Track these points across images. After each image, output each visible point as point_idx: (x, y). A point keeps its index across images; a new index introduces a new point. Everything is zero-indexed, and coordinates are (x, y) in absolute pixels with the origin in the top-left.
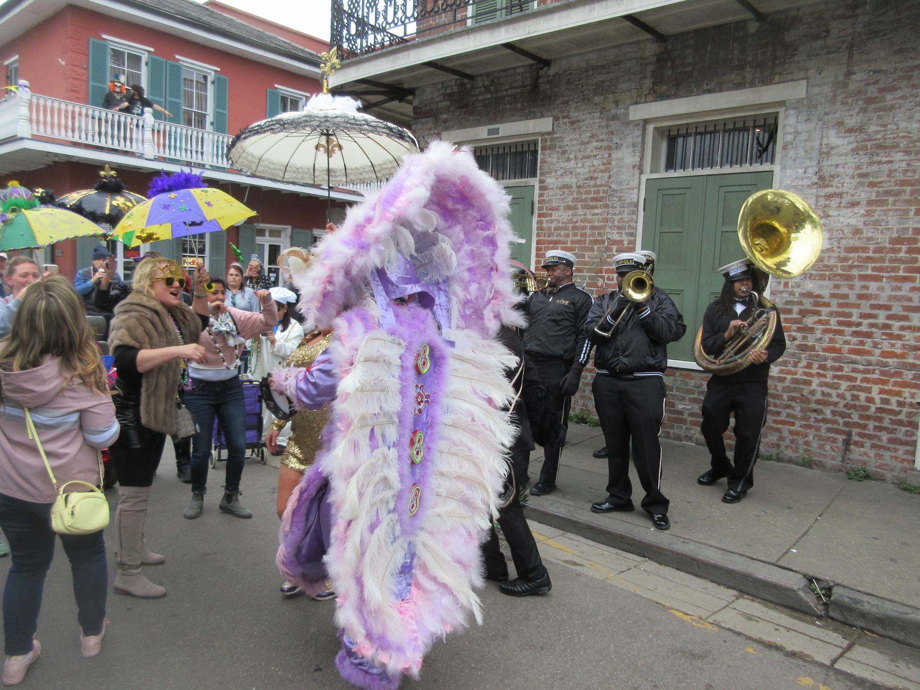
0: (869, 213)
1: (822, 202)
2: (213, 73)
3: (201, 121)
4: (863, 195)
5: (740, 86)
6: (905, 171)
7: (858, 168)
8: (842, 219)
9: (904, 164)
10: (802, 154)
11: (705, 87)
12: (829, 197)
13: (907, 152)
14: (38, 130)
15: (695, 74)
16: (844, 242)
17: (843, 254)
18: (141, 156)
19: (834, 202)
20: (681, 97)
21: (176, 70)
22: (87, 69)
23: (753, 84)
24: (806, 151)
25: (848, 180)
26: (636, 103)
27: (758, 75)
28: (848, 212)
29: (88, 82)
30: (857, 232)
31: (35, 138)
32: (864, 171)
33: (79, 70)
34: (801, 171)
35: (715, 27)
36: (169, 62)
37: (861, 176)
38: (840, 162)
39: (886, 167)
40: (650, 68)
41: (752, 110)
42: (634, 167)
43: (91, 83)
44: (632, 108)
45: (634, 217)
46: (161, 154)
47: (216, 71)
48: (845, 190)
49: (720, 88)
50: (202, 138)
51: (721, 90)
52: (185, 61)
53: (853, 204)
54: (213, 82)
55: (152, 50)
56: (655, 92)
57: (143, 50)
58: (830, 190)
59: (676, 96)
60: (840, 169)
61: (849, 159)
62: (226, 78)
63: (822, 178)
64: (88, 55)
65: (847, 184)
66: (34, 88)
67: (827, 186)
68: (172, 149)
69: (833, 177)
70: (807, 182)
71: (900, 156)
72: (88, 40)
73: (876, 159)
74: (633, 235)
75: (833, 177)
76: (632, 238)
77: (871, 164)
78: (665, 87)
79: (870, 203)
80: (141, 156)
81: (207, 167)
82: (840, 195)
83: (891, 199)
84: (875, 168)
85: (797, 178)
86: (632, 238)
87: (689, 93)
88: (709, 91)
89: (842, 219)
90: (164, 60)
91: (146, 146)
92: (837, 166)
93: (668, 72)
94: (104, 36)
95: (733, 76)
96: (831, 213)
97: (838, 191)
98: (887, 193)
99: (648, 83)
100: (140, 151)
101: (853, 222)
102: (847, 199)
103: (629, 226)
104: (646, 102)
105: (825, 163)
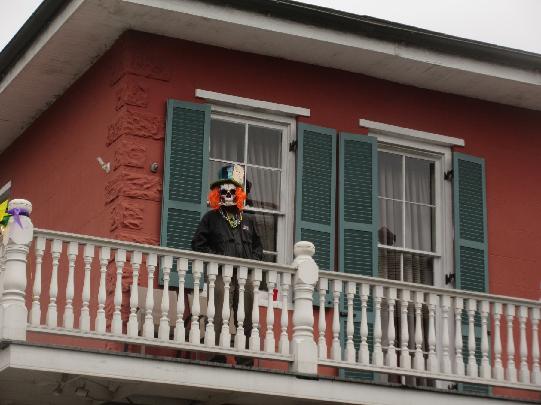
2: (447, 154)
3: (422, 268)
14: (44, 320)
18: (284, 369)
21: (362, 154)
22: (159, 171)
29: (160, 201)
31: (37, 340)
33: (142, 176)
36: (344, 136)
43: (168, 204)
46: (337, 361)
47: (453, 148)
50: (425, 310)
52: (384, 132)
54: (449, 176)
55: (305, 112)
57: (284, 117)
62: (481, 161)
64: (163, 140)
66: (39, 218)
68: (364, 346)
72: (165, 106)
80: (284, 369)
81: (439, 385)
90: (332, 132)
91: (298, 340)
94: (200, 93)
100: (285, 355)
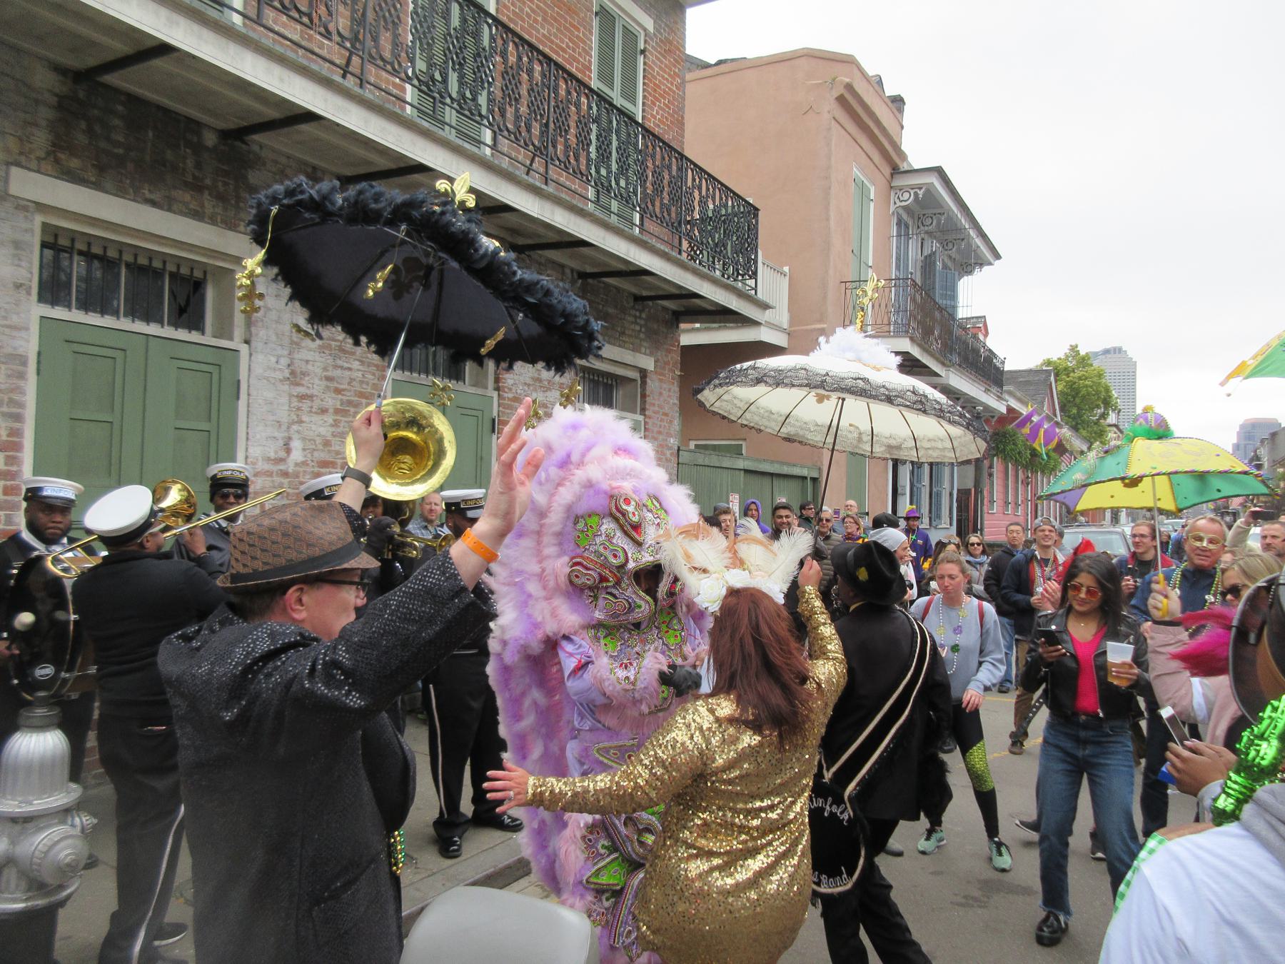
0: (336, 424)
1: (295, 403)
4: (331, 401)
5: (197, 215)
6: (362, 382)
7: (325, 369)
8: (314, 427)
9: (360, 374)
10: (274, 338)
11: (148, 195)
12: (302, 397)
13: (362, 363)
15: (130, 166)
16: (316, 454)
17: (316, 469)
19: (306, 405)
20: (107, 192)
23: (213, 221)
24: (277, 335)
25: (317, 381)
26: (18, 165)
27: (219, 210)
28: (315, 418)
30: (327, 443)
32: (329, 374)
34: (273, 359)
35: (159, 108)
37: (329, 379)
38: (310, 358)
39: (347, 373)
40: (45, 114)
41: (203, 255)
42: (18, 286)
44: (15, 171)
45: (22, 383)
48: (315, 392)
49: (167, 205)
51: (169, 210)
53: (324, 411)
56: (57, 161)
58: (301, 390)
59: (97, 186)
60: (310, 367)
61: (317, 356)
63: (293, 373)
65: (315, 385)
67: (298, 384)
69: (304, 374)
70: (279, 375)
71: (356, 365)
73: (339, 362)
74: (18, 418)
75: (304, 374)
76: (17, 425)
77: (336, 367)
78: (74, 163)
79: (337, 411)
82: (310, 397)
83: (352, 410)
84: (338, 373)
85: (269, 368)
86: (17, 425)
87: (121, 192)
88: (153, 203)
89: (314, 427)
92: (307, 362)
93: (81, 139)
95: (187, 197)
96: (305, 418)
97: (309, 392)
98: (350, 403)
99: (41, 139)
101: (323, 431)
102: (317, 403)
103: (11, 401)
104: (38, 172)
105: (296, 356)
